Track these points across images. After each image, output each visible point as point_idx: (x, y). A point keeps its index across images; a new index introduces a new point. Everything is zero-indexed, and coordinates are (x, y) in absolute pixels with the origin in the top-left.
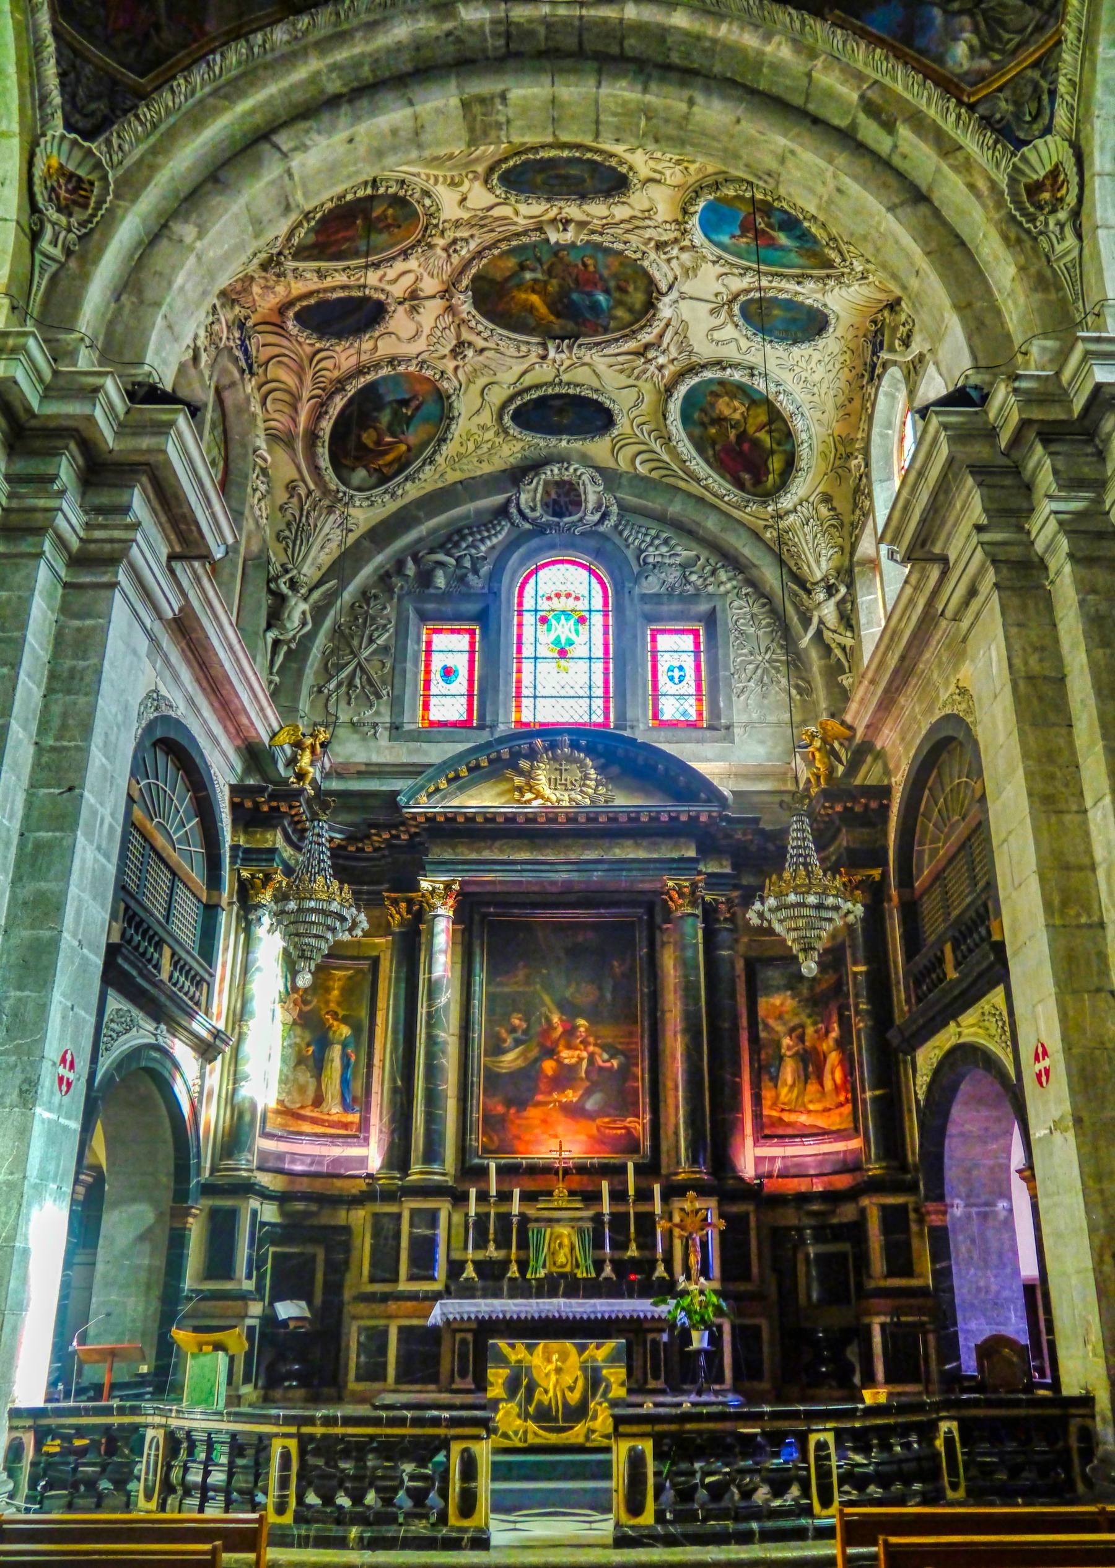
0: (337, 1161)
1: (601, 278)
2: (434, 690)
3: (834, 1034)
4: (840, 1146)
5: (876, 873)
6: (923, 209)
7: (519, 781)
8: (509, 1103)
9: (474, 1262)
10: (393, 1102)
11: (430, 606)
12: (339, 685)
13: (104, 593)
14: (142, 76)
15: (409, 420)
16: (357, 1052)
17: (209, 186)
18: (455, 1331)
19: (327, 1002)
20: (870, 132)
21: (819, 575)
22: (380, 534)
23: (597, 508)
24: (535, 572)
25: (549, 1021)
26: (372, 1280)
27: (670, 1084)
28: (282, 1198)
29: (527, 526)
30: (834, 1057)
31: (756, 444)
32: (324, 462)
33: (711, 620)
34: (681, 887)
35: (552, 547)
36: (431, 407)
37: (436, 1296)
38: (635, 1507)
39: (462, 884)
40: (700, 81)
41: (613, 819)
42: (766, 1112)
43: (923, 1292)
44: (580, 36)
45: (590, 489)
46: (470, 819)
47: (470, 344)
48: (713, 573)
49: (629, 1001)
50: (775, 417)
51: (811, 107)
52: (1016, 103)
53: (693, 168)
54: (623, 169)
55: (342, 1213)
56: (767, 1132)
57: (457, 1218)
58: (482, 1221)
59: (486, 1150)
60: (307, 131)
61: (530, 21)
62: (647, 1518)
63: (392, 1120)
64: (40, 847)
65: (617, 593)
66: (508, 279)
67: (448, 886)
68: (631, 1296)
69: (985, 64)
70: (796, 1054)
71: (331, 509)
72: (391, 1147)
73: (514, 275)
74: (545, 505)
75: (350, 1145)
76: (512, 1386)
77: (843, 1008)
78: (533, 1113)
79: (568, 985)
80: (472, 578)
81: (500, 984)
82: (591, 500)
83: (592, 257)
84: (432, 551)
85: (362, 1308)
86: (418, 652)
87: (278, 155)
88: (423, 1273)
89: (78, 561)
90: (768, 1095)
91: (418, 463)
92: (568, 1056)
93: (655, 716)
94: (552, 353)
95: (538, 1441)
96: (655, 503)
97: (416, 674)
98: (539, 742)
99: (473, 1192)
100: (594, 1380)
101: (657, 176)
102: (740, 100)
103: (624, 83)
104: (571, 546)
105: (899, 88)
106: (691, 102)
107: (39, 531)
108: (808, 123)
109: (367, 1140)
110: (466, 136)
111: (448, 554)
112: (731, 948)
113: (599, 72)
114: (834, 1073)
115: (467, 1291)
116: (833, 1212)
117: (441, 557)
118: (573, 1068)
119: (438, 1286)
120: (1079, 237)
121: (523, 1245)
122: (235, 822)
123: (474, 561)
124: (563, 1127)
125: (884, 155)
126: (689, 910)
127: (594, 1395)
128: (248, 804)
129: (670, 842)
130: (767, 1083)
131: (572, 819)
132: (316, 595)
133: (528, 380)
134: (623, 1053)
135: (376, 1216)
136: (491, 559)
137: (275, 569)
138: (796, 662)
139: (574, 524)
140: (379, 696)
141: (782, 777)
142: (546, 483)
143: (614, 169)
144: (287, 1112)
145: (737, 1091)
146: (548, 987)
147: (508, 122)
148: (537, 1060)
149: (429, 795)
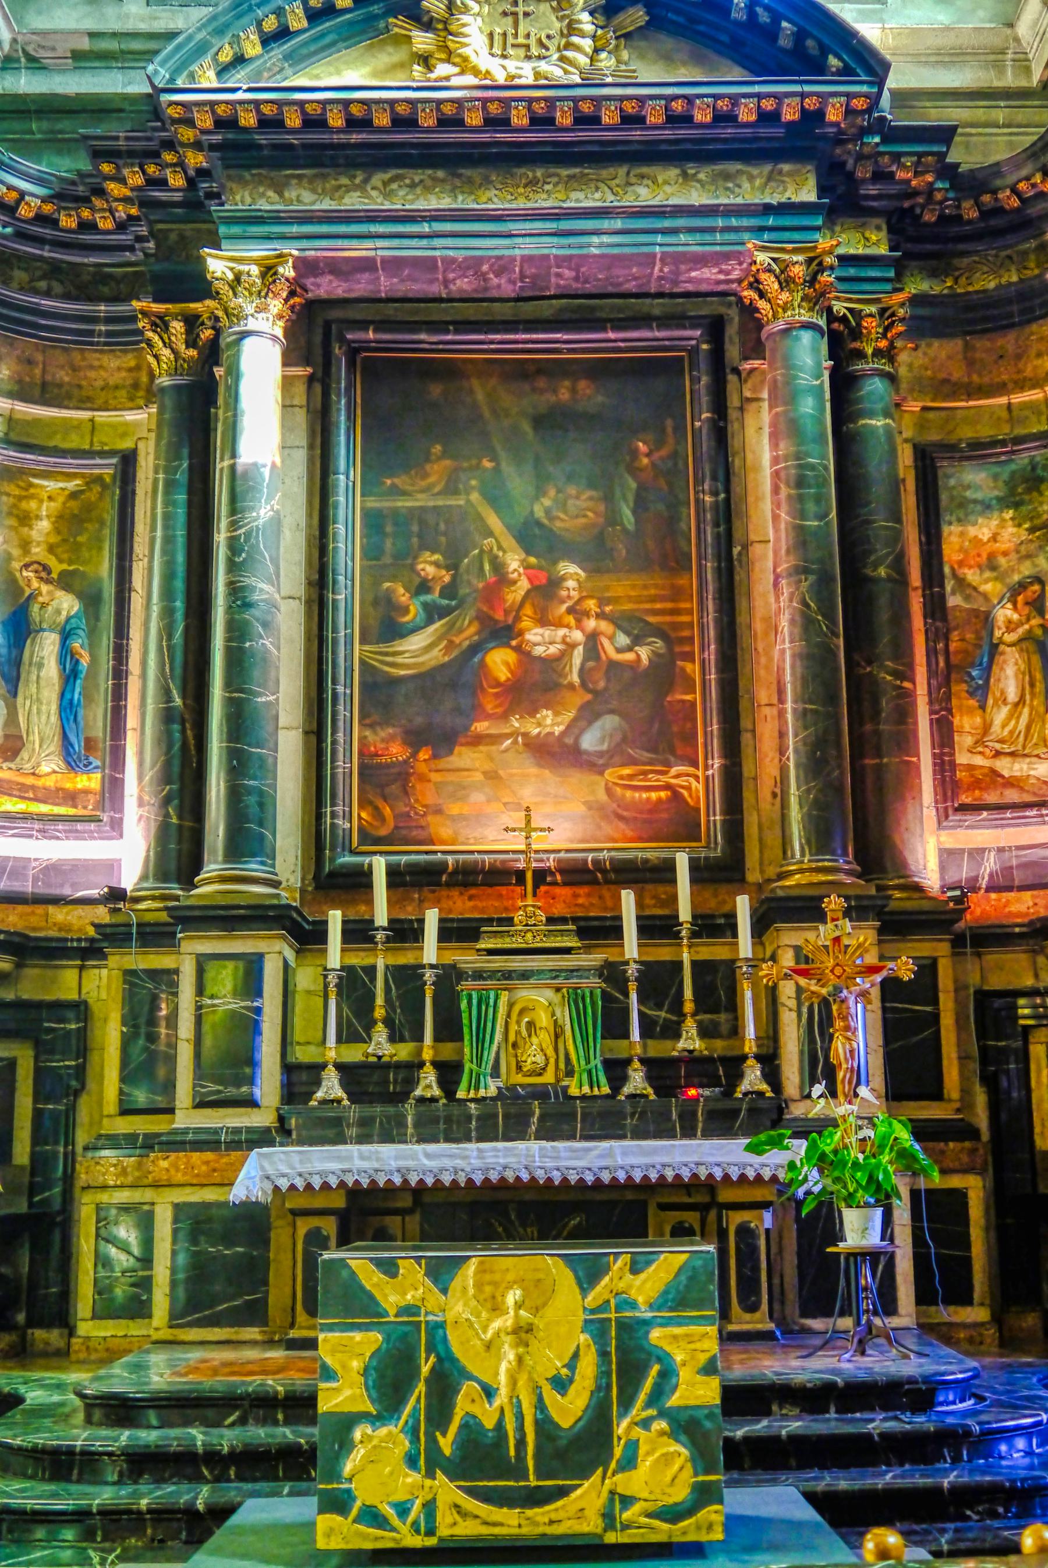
0: (53, 869)
7: (422, 40)
8: (416, 739)
9: (340, 1067)
10: (165, 739)
16: (93, 648)
18: (296, 1213)
19: (25, 545)
25: (498, 567)
27: (764, 695)
34: (785, 267)
37: (261, 1138)
39: (306, 267)
42: (962, 758)
49: (671, 523)
55: (70, 976)
56: (965, 799)
57: (306, 978)
59: (366, 837)
63: (165, 777)
67: (269, 271)
68: (689, 1132)
70: (1028, 637)
72: (163, 833)
75: (79, 836)
78: (464, 757)
79: (540, 492)
81: (397, 492)
88: (231, 1092)
90: (966, 723)
95: (467, 1529)
99: (335, 919)
109: (117, 827)
112: (887, 414)
118: (553, 665)
119: (263, 1118)
127: (626, 1403)
131: (541, 121)
134: (659, 632)
135: (130, 974)
145: (905, 713)
146: (496, 499)
148: (475, 649)
149: (223, 71)
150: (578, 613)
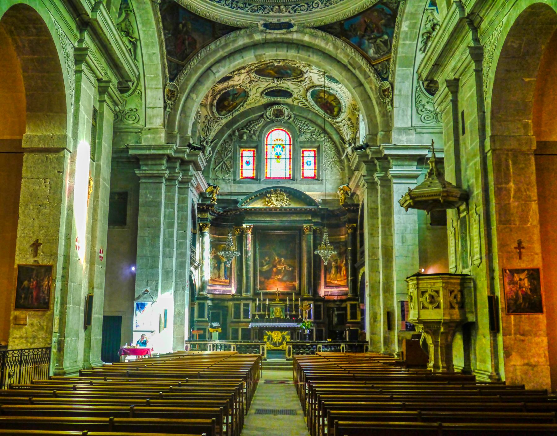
0: (224, 291)
2: (244, 168)
3: (344, 262)
4: (344, 289)
5: (355, 225)
6: (362, 88)
7: (267, 199)
8: (265, 278)
11: (242, 145)
12: (219, 168)
13: (186, 190)
14: (183, 61)
15: (237, 98)
17: (198, 84)
21: (347, 139)
22: (228, 125)
23: (288, 116)
24: (271, 132)
25: (275, 259)
26: (235, 318)
28: (212, 300)
29: (269, 120)
30: (344, 268)
31: (331, 104)
32: (214, 109)
33: (318, 148)
35: (276, 126)
36: (243, 94)
37: (249, 322)
38: (289, 355)
40: (311, 50)
41: (291, 210)
43: (358, 323)
45: (286, 111)
46: (255, 210)
47: (254, 81)
48: (320, 134)
50: (336, 99)
52: (382, 68)
57: (254, 305)
58: (260, 305)
59: (260, 289)
60: (219, 67)
62: (291, 357)
64: (181, 243)
65: (293, 140)
67: (250, 227)
69: (376, 56)
71: (216, 122)
74: (274, 115)
76: (268, 339)
77: (346, 257)
80: (253, 136)
82: (286, 113)
84: (242, 129)
85: (232, 324)
86: (239, 158)
87: (212, 74)
89: (180, 183)
90: (328, 276)
91: (239, 107)
92: (279, 267)
93: (303, 176)
94: (276, 82)
96: (305, 115)
97: (239, 164)
98: (272, 190)
100: (284, 338)
102: (321, 55)
103: (293, 51)
104: (281, 125)
105: (357, 59)
106: (309, 56)
107: (175, 180)
108: (336, 63)
109: (231, 286)
111: (247, 130)
113: (287, 48)
114: (343, 272)
115: (257, 321)
116: (341, 304)
117: (245, 130)
118: (280, 270)
119: (250, 320)
120: (392, 106)
121: (269, 311)
122: (198, 211)
123: (254, 131)
124: (278, 283)
126: (309, 233)
128: (201, 207)
129: (304, 215)
130: (328, 273)
131: (280, 210)
132: (212, 144)
133: (269, 86)
135: (235, 304)
136: (259, 130)
137: (202, 139)
138: (341, 162)
139: (281, 120)
140: (230, 171)
141: (335, 196)
142: (274, 110)
144: (212, 280)
150: (283, 264)
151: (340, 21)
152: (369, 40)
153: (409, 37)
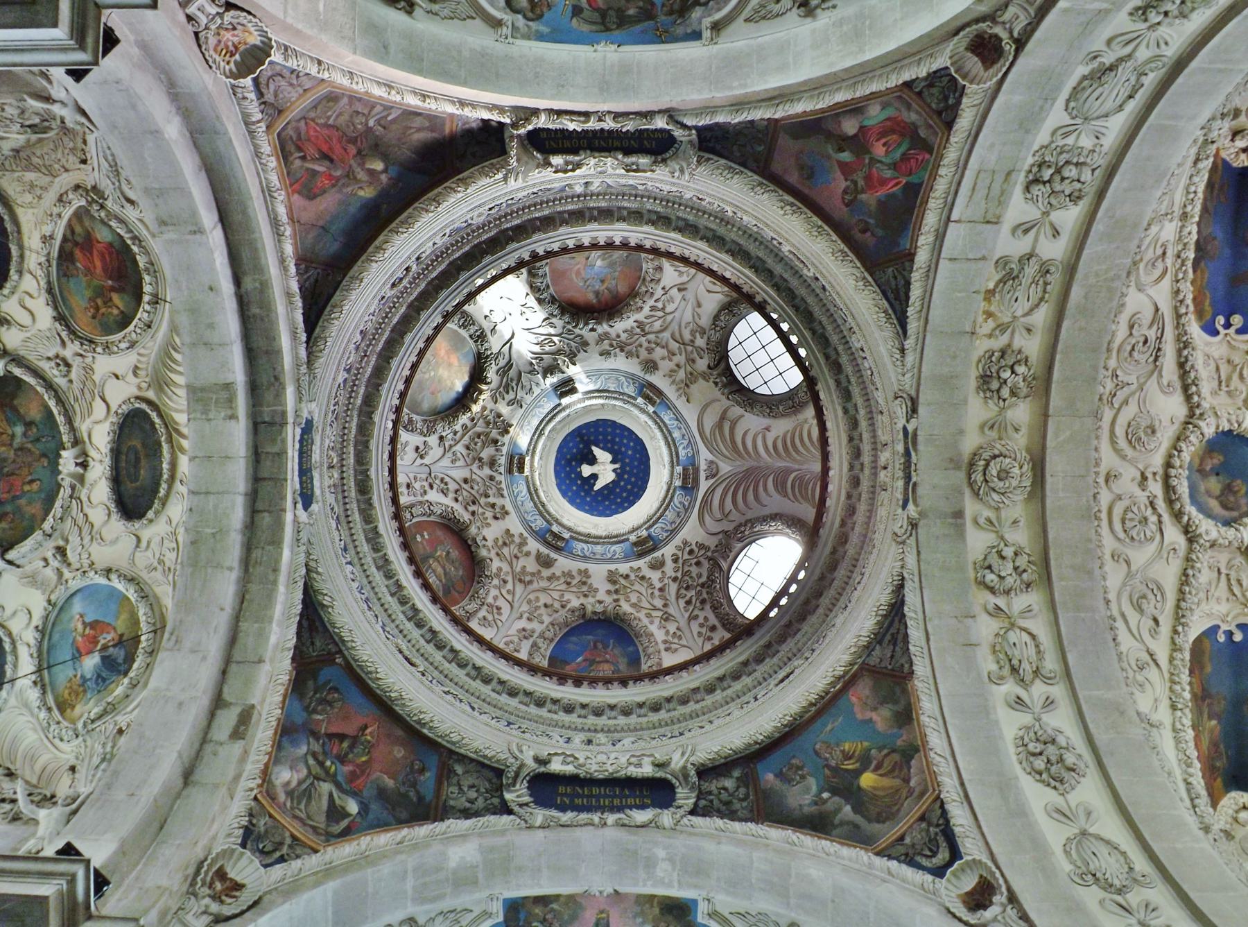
1: (15, 498)
20: (227, 719)
44: (270, 479)
51: (233, 668)
52: (266, 832)
53: (158, 575)
54: (150, 514)
61: (284, 441)
66: (15, 410)
69: (282, 797)
73: (20, 418)
83: (40, 491)
101: (144, 544)
102: (234, 609)
110: (198, 384)
125: (209, 736)
143: (150, 508)
147: (209, 420)
151: (340, 652)
152: (314, 755)
153: (427, 879)
